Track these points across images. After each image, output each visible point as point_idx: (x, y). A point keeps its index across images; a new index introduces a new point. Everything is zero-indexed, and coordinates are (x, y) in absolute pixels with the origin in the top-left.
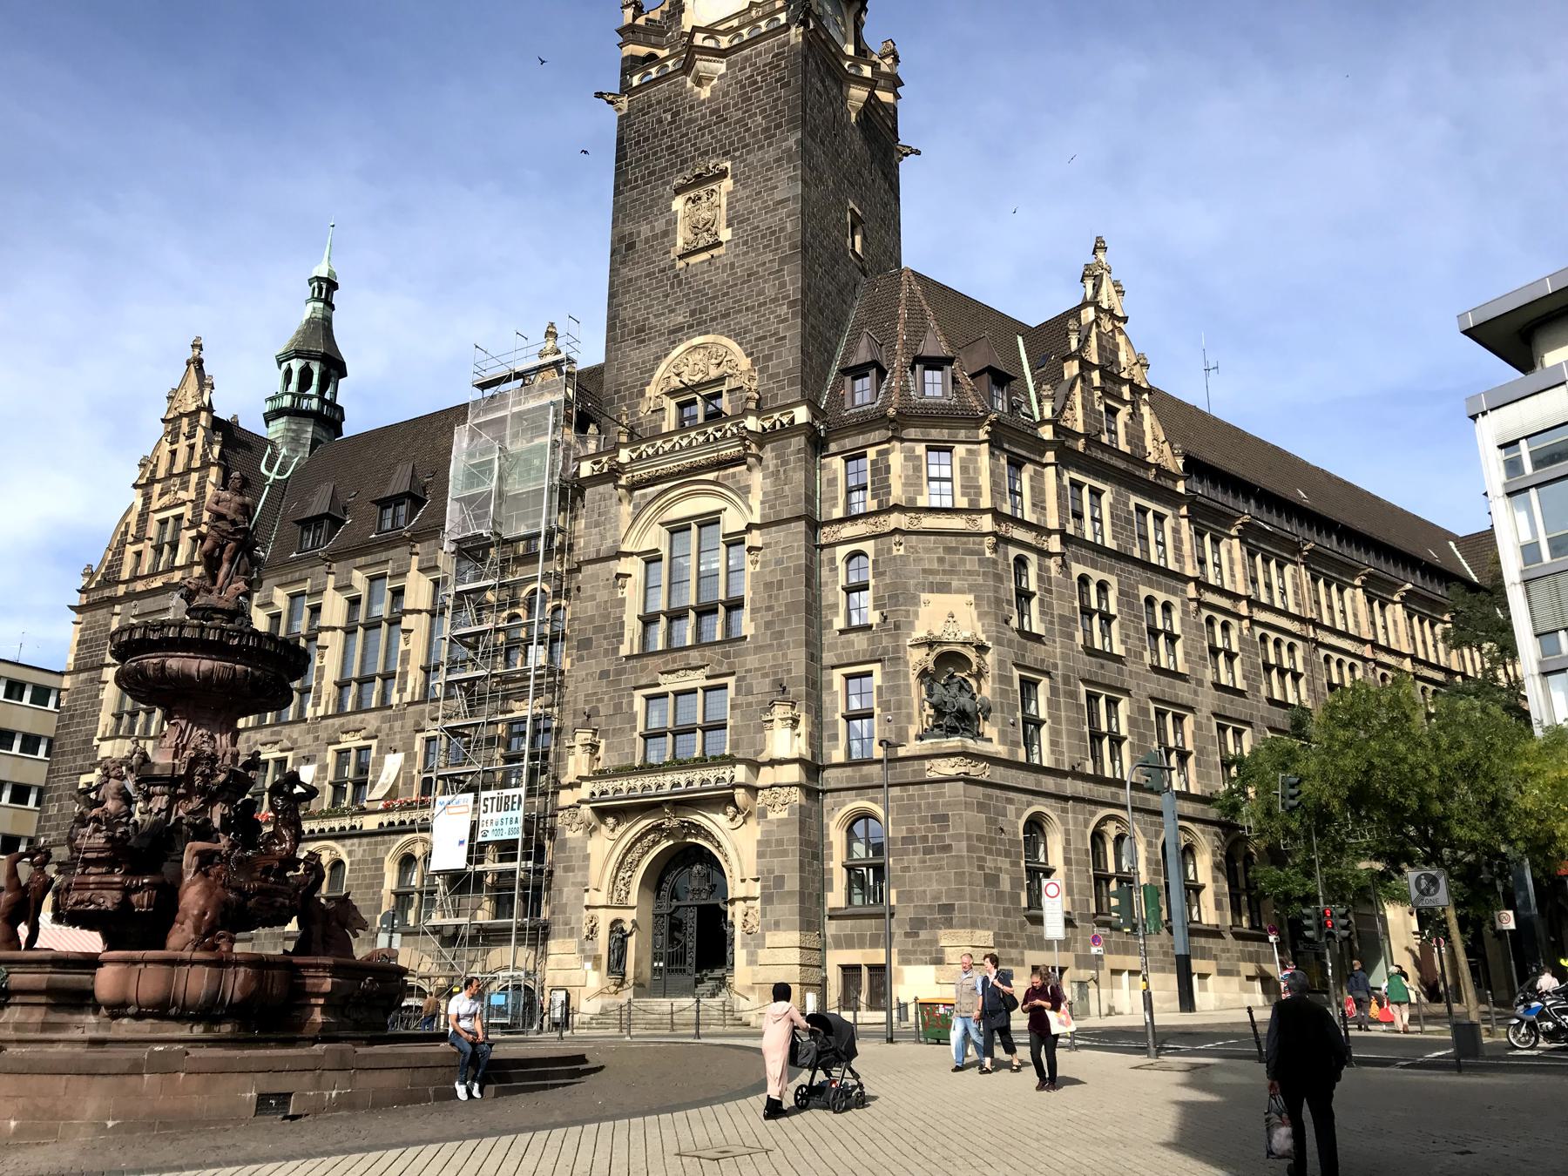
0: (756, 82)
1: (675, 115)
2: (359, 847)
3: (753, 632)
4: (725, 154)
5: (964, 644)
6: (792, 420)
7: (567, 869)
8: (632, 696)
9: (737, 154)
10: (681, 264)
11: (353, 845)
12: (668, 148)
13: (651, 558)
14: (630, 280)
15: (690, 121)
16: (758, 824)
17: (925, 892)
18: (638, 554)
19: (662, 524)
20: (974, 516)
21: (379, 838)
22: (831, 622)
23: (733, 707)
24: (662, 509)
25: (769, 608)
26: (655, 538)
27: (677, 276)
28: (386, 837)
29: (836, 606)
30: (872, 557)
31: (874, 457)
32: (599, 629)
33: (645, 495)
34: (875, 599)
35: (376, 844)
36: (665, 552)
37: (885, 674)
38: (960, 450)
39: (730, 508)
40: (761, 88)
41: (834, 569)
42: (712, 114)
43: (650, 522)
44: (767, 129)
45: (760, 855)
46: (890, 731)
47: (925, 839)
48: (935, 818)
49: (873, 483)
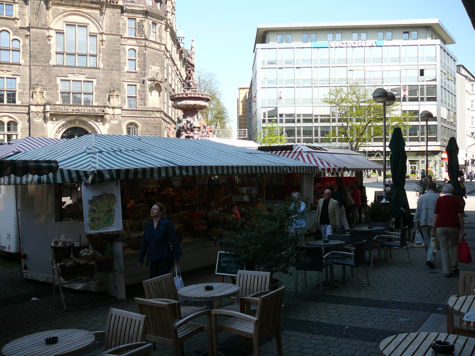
3: (102, 67)
5: (160, 82)
6: (117, 3)
8: (56, 78)
13: (59, 32)
16: (108, 124)
18: (55, 30)
19: (65, 22)
20: (161, 45)
22: (124, 68)
24: (64, 16)
25: (108, 61)
26: (60, 25)
29: (125, 63)
30: (137, 51)
31: (139, 21)
33: (58, 9)
34: (138, 64)
36: (65, 31)
37: (141, 87)
38: (158, 25)
39: (91, 24)
41: (125, 52)
43: (59, 19)
48: (153, 127)
49: (138, 29)
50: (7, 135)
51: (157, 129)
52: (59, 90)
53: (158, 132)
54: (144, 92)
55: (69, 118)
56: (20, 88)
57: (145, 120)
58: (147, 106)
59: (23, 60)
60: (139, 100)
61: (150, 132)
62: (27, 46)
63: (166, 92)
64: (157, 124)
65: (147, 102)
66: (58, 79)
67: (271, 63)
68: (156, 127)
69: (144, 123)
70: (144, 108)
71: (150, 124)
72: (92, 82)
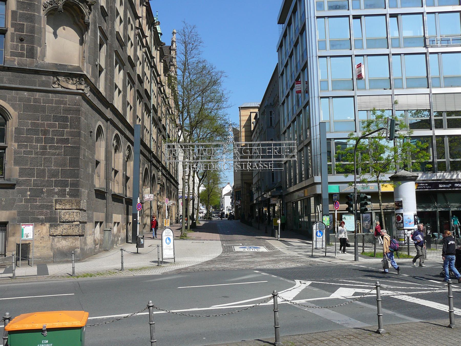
17: (44, 170)
46: (22, 49)
48: (56, 119)
51: (65, 127)
53: (71, 134)
54: (31, 19)
57: (29, 100)
58: (40, 62)
60: (12, 40)
61: (45, 132)
63: (105, 46)
64: (67, 110)
65: (39, 48)
67: (337, 7)
68: (65, 119)
69: (27, 108)
70: (27, 62)
71: (44, 112)
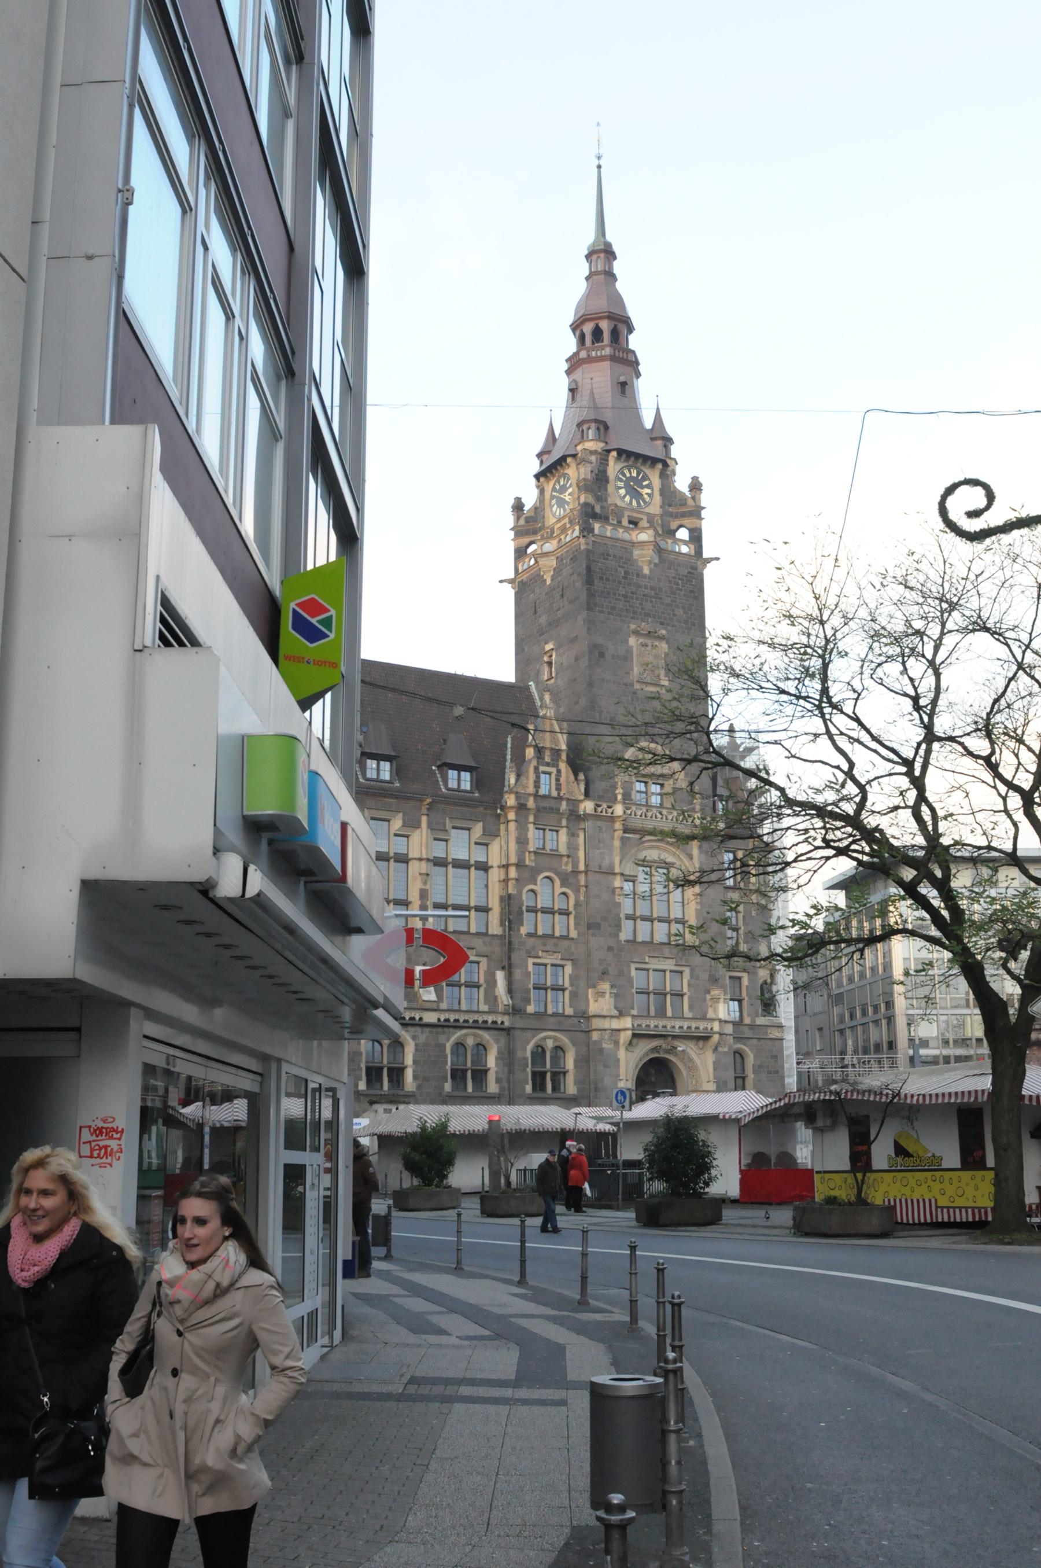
0: (677, 584)
1: (627, 573)
2: (423, 1035)
4: (662, 624)
7: (606, 1066)
8: (630, 967)
9: (669, 628)
10: (637, 686)
11: (416, 1032)
12: (625, 596)
14: (603, 680)
15: (638, 586)
21: (440, 1029)
23: (689, 985)
27: (635, 693)
28: (446, 1029)
32: (604, 919)
35: (437, 1033)
37: (750, 980)
40: (681, 590)
42: (652, 588)
44: (686, 622)
45: (715, 1069)
47: (768, 1067)
50: (551, 1072)
52: (635, 986)
55: (655, 1043)
56: (571, 985)
59: (576, 932)
62: (581, 905)
66: (633, 966)
72: (681, 972)
